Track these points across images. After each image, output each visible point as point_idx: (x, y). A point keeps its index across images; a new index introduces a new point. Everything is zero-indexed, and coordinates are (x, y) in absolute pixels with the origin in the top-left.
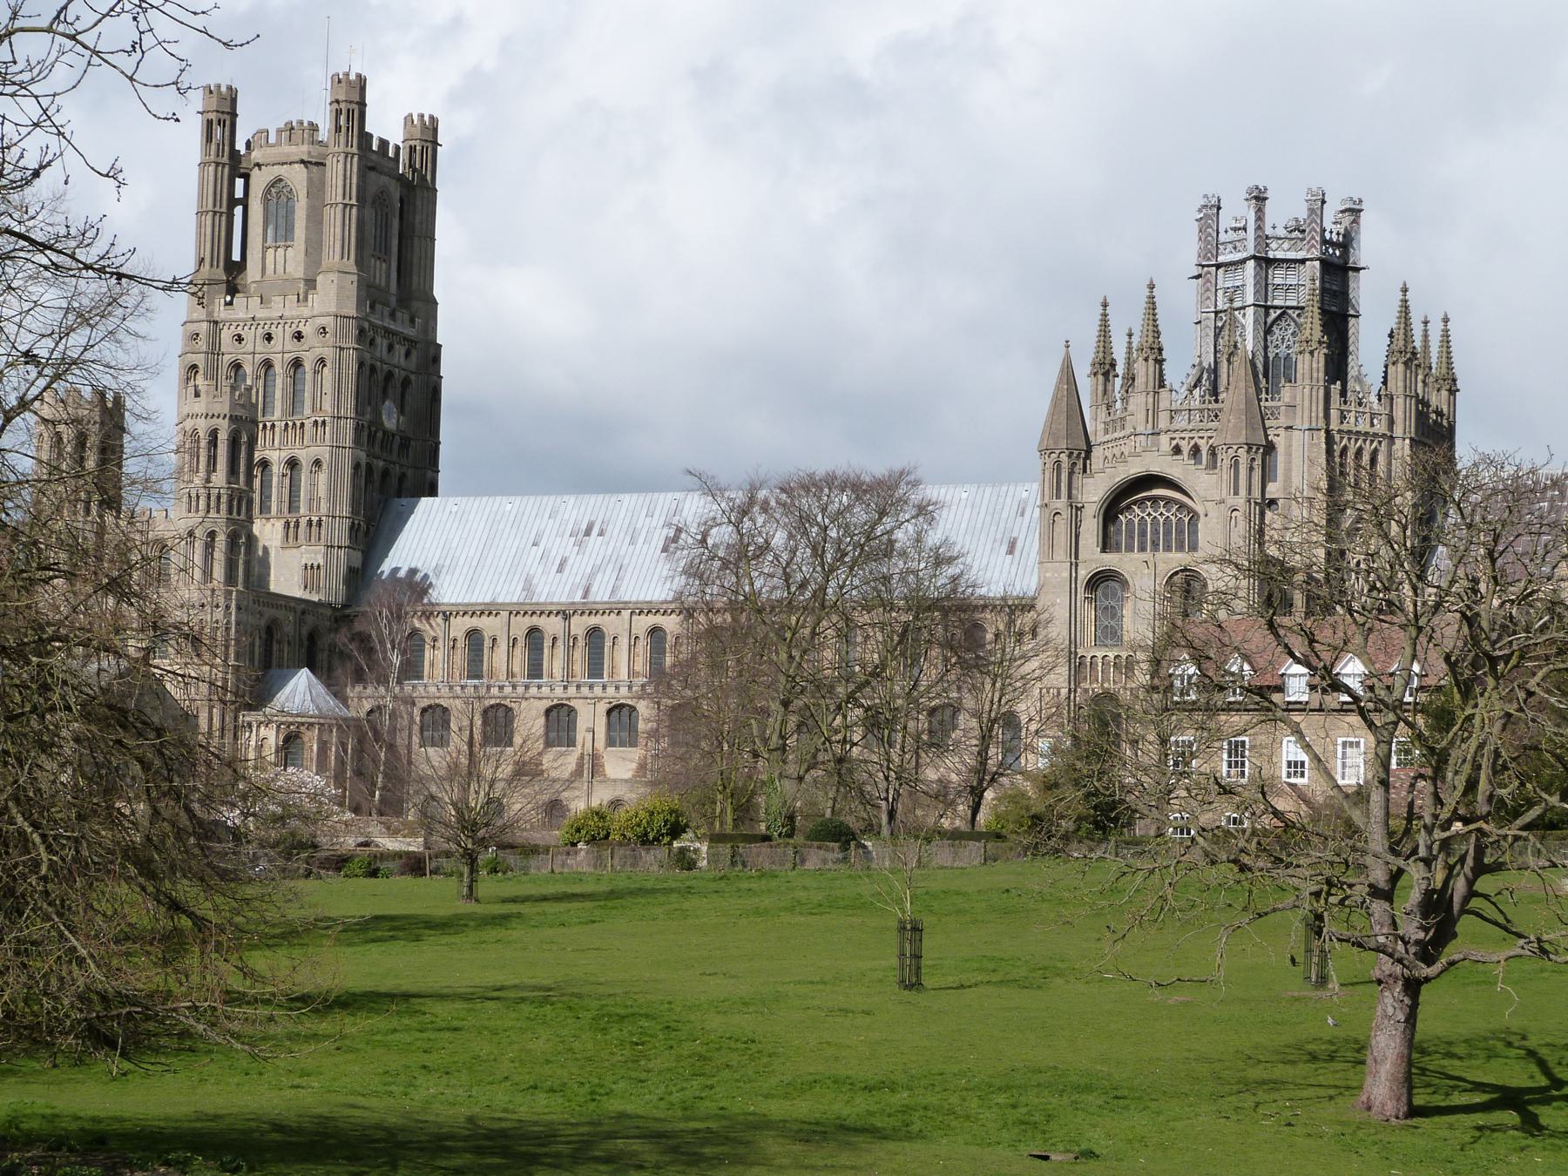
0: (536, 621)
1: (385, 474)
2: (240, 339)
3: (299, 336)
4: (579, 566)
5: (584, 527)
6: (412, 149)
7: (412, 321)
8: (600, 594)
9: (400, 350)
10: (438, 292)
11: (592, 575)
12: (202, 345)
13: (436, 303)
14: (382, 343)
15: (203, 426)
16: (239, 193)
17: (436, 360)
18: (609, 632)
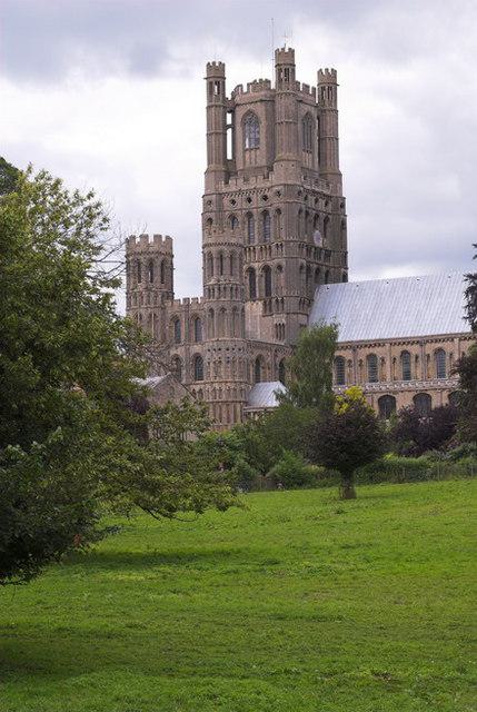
1: (318, 271)
2: (233, 202)
3: (265, 198)
6: (323, 89)
9: (322, 202)
10: (342, 169)
12: (213, 207)
13: (341, 175)
14: (312, 199)
15: (214, 250)
16: (229, 121)
17: (343, 206)
18: (448, 351)
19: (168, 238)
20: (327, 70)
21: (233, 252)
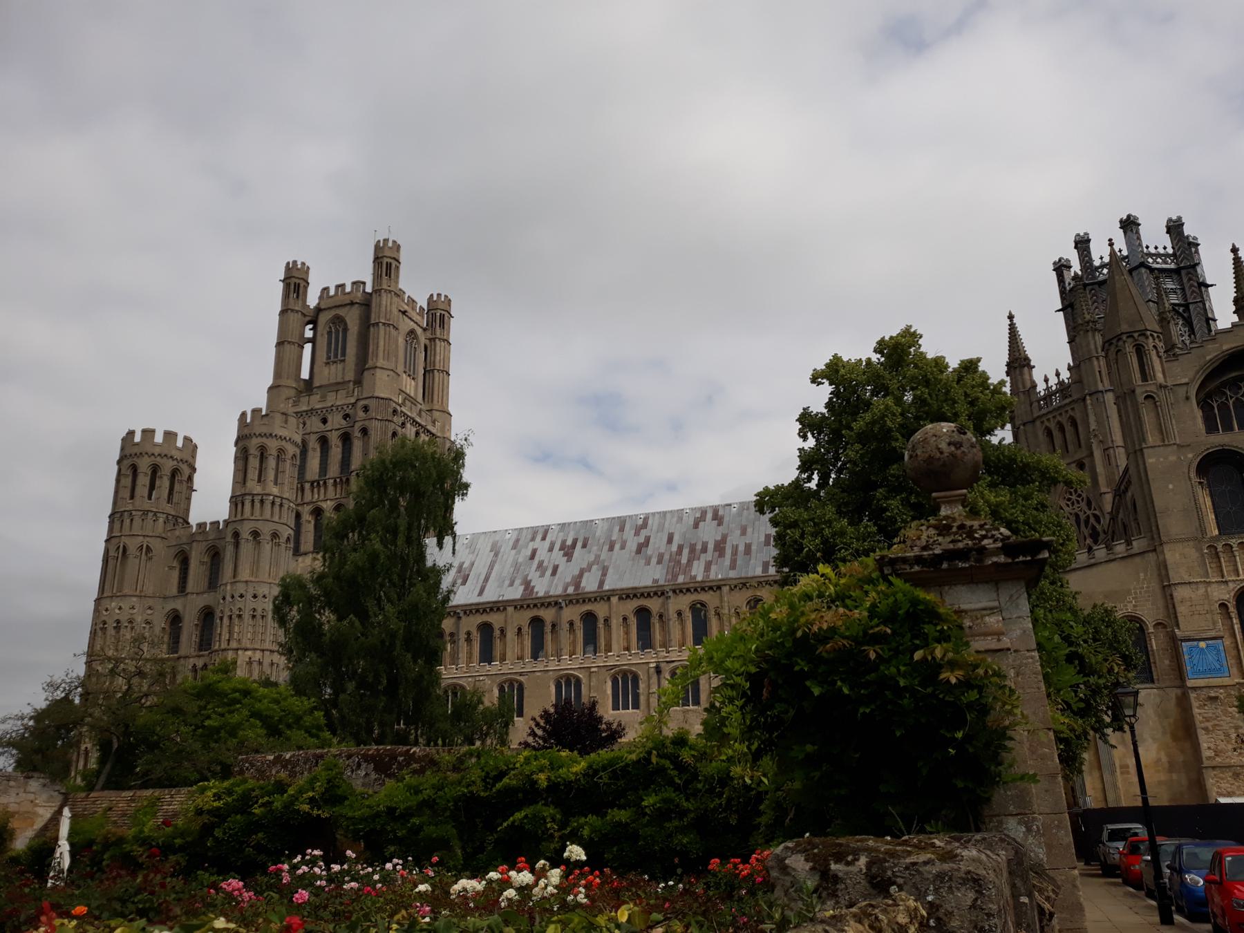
0: (535, 612)
4: (568, 571)
5: (569, 542)
7: (434, 422)
8: (590, 584)
11: (581, 575)
19: (187, 440)
20: (439, 295)
21: (281, 451)
